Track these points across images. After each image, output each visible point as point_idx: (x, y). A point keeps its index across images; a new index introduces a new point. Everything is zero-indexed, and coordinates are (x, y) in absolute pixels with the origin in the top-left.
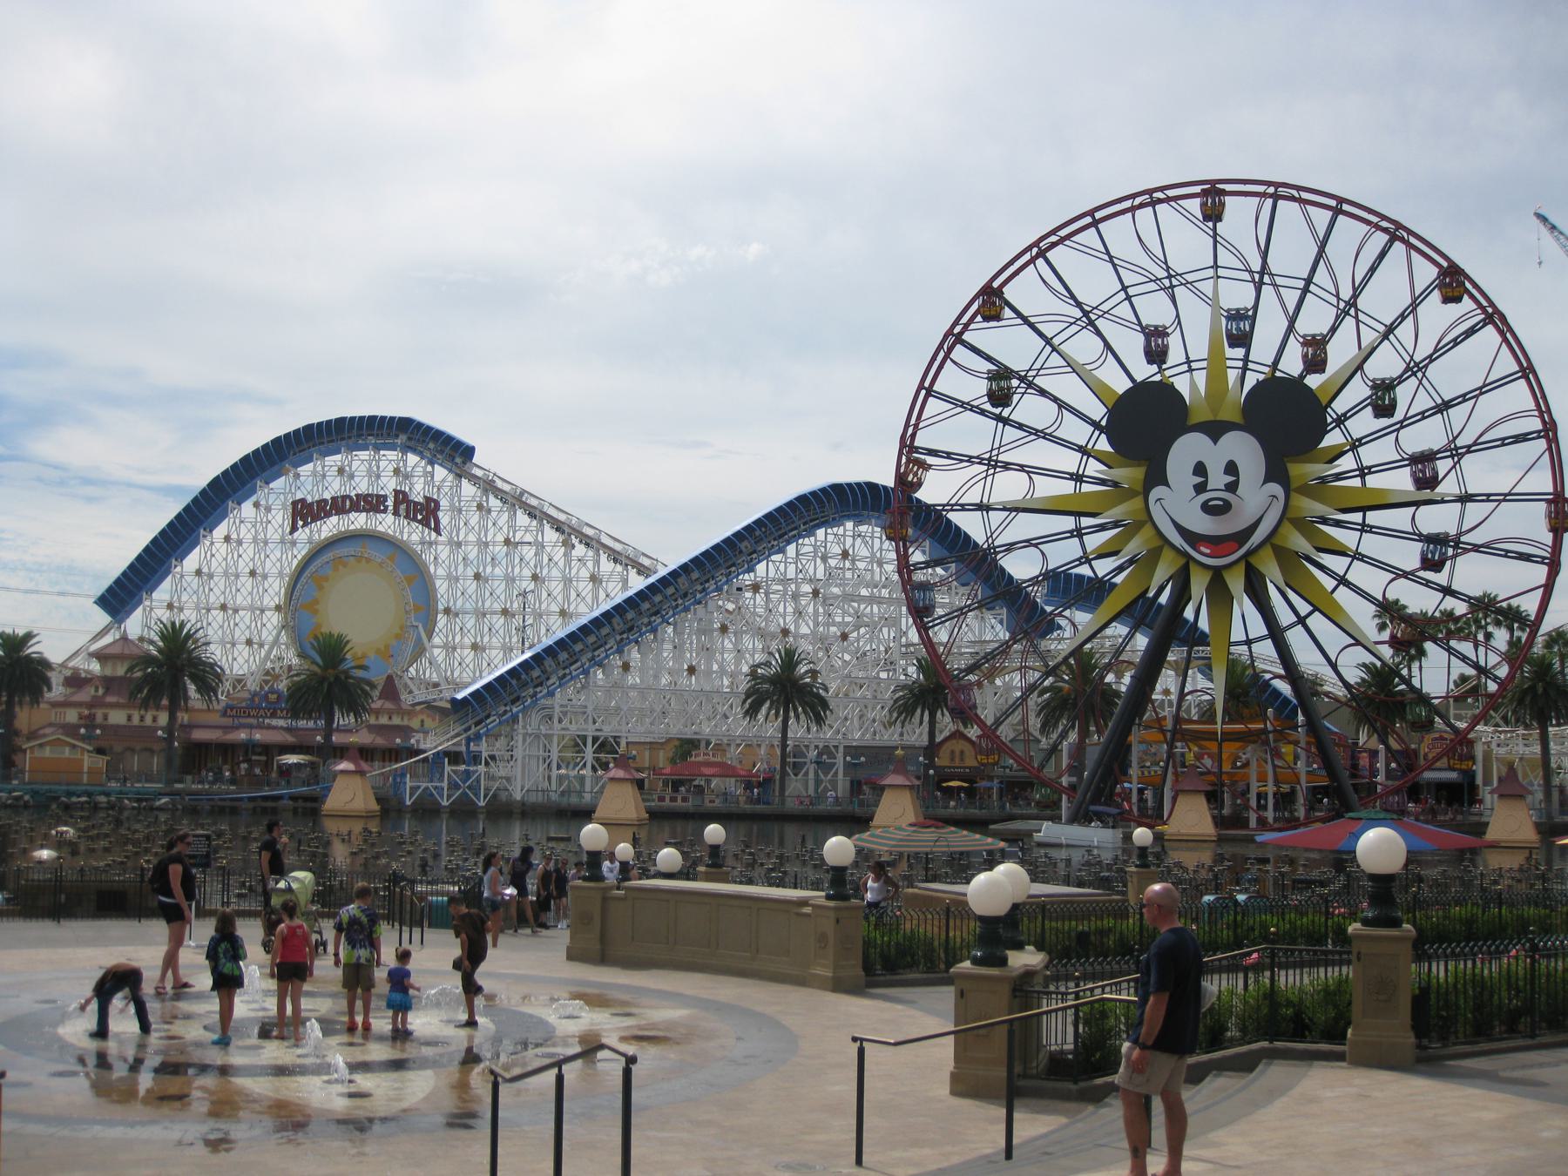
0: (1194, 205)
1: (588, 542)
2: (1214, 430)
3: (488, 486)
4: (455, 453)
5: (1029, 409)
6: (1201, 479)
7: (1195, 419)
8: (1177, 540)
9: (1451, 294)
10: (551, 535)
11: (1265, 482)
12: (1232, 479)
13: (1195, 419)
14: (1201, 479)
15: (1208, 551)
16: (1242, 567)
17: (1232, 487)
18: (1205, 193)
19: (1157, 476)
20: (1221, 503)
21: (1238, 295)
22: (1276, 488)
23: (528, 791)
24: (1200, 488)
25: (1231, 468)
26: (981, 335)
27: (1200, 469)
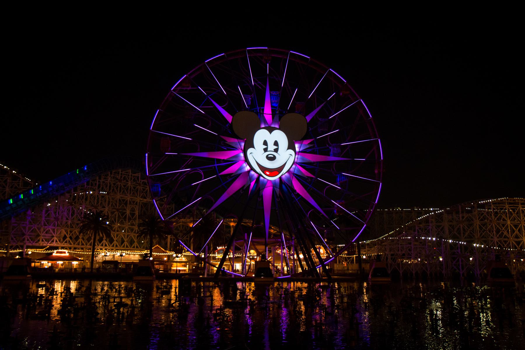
6: (266, 147)
9: (345, 93)
11: (288, 149)
12: (276, 147)
14: (266, 147)
15: (268, 173)
17: (276, 150)
22: (291, 152)
25: (276, 143)
27: (265, 143)
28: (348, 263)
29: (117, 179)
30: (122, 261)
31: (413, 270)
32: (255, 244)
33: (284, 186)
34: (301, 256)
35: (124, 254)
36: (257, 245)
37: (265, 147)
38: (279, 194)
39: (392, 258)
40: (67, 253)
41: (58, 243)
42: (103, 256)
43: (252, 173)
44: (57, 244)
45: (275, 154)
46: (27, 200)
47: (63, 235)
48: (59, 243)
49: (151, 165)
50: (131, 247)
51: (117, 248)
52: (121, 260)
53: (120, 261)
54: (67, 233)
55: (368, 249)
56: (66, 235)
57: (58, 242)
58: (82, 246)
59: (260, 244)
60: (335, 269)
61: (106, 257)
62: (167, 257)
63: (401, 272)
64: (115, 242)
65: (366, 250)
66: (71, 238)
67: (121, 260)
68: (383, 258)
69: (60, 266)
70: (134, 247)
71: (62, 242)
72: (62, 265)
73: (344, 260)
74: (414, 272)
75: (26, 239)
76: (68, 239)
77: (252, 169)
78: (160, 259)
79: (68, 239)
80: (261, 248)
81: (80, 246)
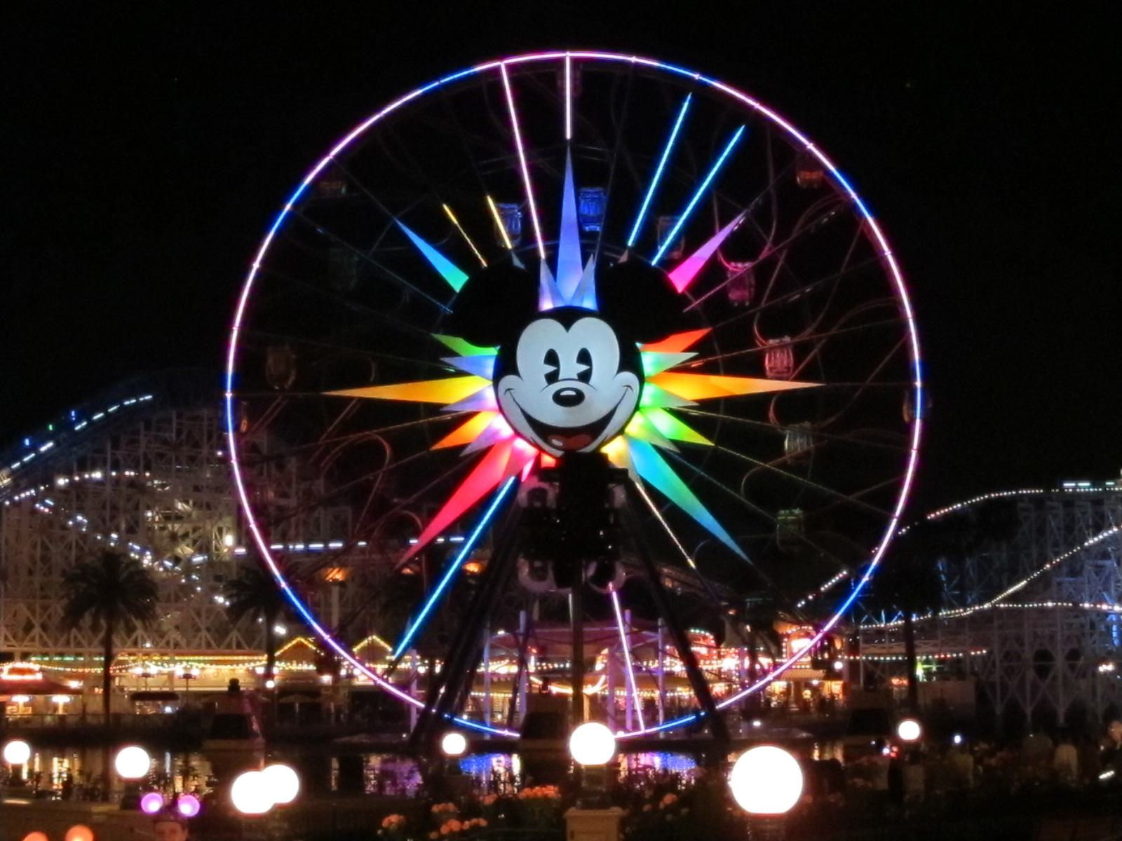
2: (567, 316)
7: (547, 305)
12: (584, 368)
13: (547, 305)
17: (585, 377)
19: (506, 366)
22: (629, 377)
24: (552, 378)
29: (165, 442)
30: (190, 689)
37: (551, 369)
41: (10, 644)
42: (139, 677)
43: (520, 444)
44: (9, 646)
45: (581, 386)
48: (13, 642)
49: (244, 428)
50: (219, 646)
51: (177, 650)
52: (187, 687)
53: (185, 689)
54: (33, 612)
55: (943, 638)
56: (31, 618)
57: (10, 641)
61: (149, 679)
65: (939, 642)
66: (44, 627)
67: (187, 687)
70: (229, 646)
71: (23, 640)
72: (26, 705)
76: (37, 631)
78: (311, 681)
79: (37, 631)
81: (72, 648)
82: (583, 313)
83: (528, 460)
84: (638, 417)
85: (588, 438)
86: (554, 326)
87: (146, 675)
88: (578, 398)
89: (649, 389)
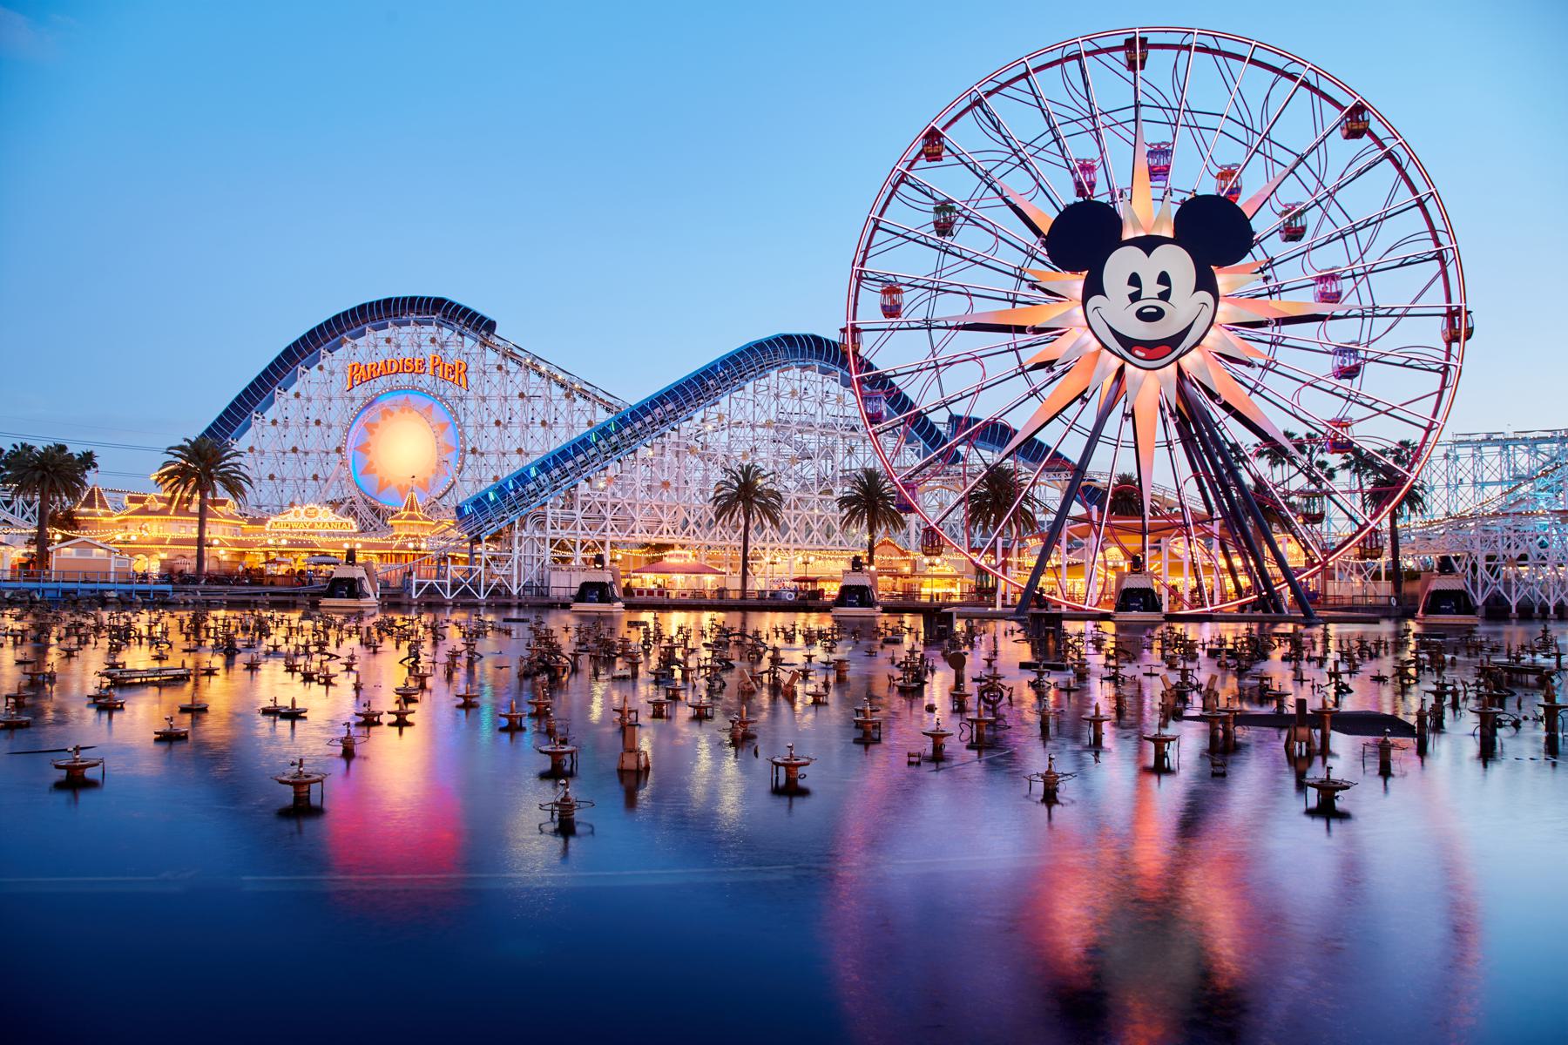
0: (1121, 55)
1: (584, 395)
2: (1148, 244)
3: (509, 355)
4: (482, 326)
5: (966, 237)
8: (1115, 345)
9: (1356, 127)
10: (558, 392)
11: (1195, 291)
13: (1128, 234)
15: (1143, 355)
16: (1172, 369)
17: (1165, 296)
18: (1130, 44)
19: (1094, 287)
20: (1155, 310)
21: (1155, 134)
22: (1205, 296)
23: (524, 587)
24: (1135, 297)
25: (1164, 279)
26: (925, 173)
27: (1134, 280)
28: (1365, 578)
31: (1548, 597)
32: (1116, 531)
33: (1187, 385)
34: (1237, 562)
35: (812, 559)
36: (1122, 534)
38: (1177, 406)
39: (1488, 567)
40: (690, 557)
45: (1161, 304)
46: (604, 446)
47: (681, 521)
58: (723, 543)
59: (1128, 530)
60: (1330, 592)
62: (909, 564)
63: (1513, 604)
64: (792, 532)
68: (1463, 565)
69: (679, 586)
73: (1354, 572)
74: (1551, 604)
75: (609, 528)
76: (691, 527)
77: (1104, 346)
80: (1133, 543)
82: (1161, 241)
83: (1110, 374)
84: (1212, 332)
85: (1170, 349)
86: (1136, 252)
87: (773, 563)
88: (1159, 314)
89: (1222, 306)
